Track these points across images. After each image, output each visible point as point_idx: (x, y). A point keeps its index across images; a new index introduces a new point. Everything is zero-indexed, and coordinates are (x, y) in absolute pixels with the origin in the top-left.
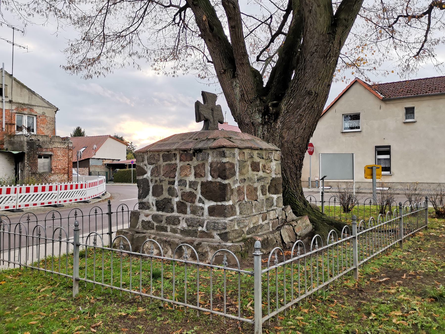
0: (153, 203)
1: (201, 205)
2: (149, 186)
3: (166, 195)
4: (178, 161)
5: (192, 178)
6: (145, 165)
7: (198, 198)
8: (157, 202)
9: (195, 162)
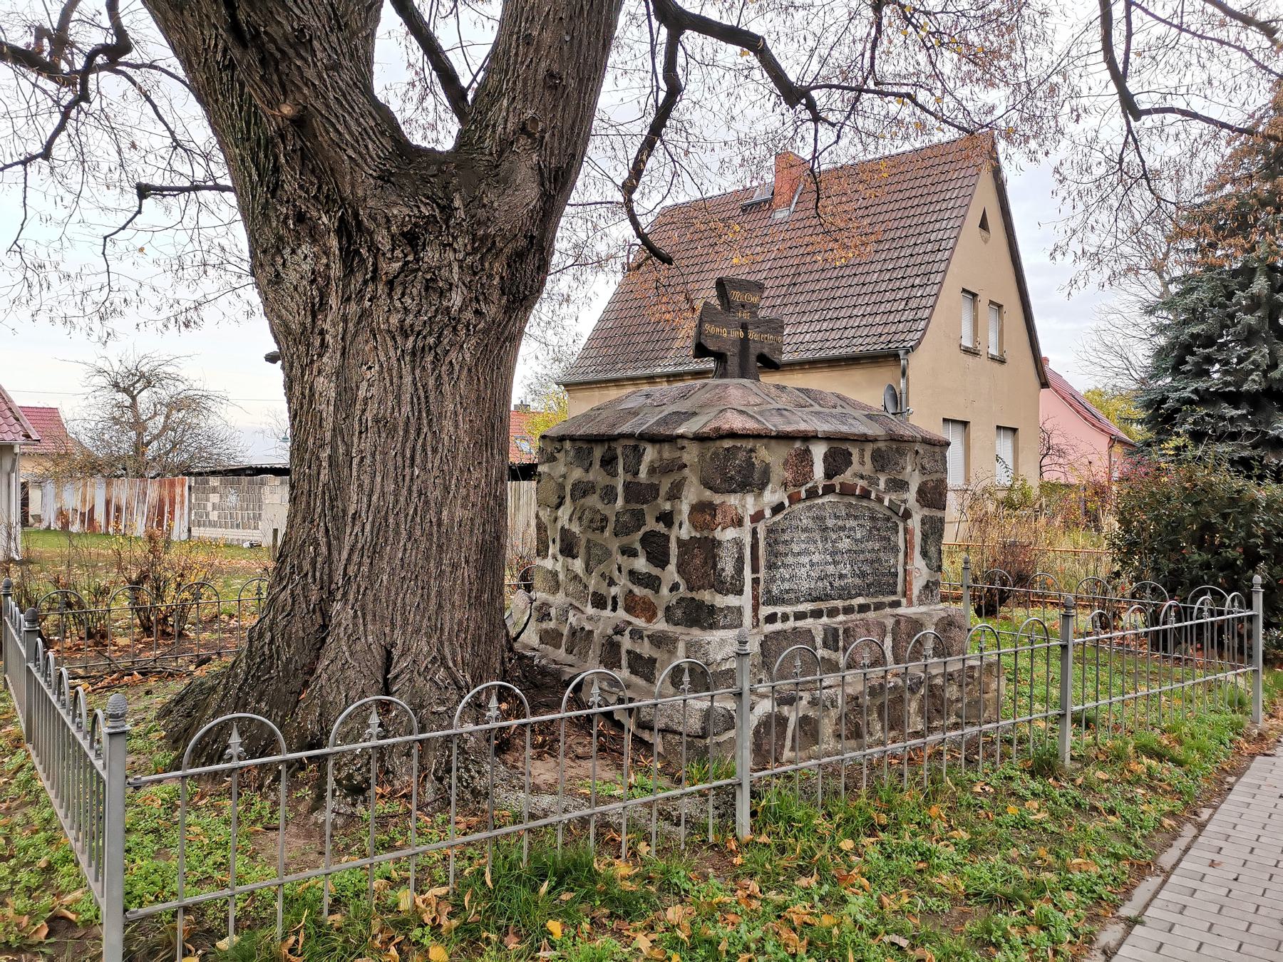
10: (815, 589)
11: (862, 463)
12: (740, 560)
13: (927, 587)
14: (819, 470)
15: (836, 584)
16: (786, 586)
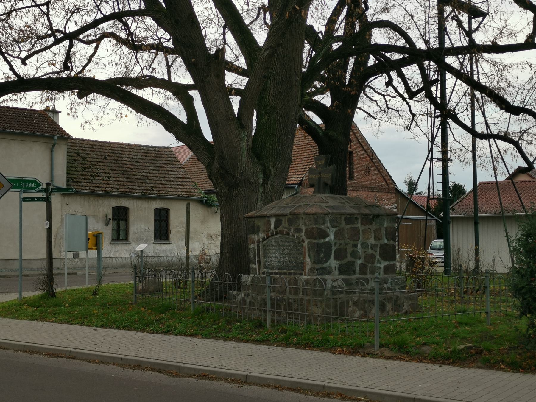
1: (378, 265)
2: (331, 250)
3: (349, 258)
4: (359, 225)
5: (372, 241)
6: (328, 228)
7: (377, 259)
8: (340, 266)
9: (374, 226)
10: (278, 265)
11: (285, 223)
12: (255, 254)
13: (311, 269)
14: (272, 226)
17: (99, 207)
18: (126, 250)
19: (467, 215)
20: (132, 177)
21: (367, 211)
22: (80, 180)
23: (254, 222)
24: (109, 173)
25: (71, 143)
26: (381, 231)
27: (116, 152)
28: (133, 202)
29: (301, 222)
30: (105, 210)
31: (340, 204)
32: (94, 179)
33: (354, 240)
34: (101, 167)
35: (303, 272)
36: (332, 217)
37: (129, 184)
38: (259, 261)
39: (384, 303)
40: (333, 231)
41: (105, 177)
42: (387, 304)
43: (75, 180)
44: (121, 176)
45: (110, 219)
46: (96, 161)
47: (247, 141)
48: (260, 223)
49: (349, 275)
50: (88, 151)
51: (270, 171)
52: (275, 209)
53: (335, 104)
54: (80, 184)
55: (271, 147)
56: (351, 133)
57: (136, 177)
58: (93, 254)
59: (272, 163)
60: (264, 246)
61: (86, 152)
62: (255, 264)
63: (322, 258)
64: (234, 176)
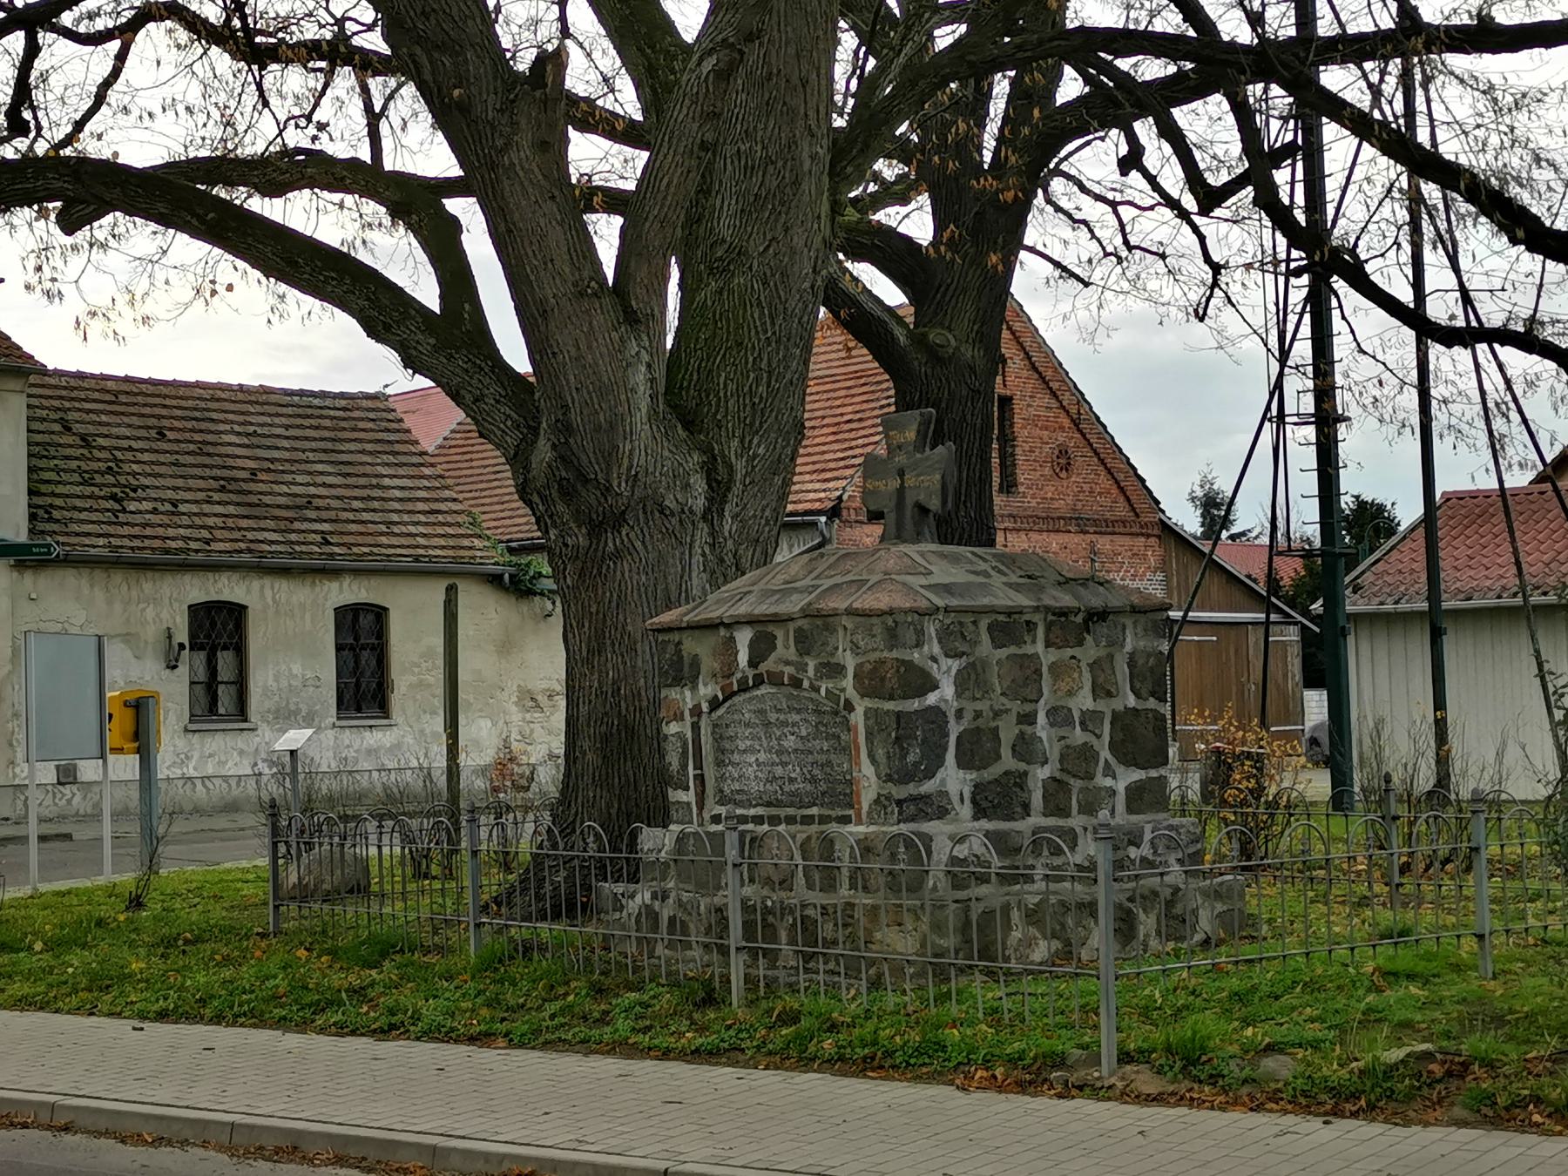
0: (961, 794)
1: (1108, 782)
2: (947, 735)
3: (1008, 761)
4: (1040, 647)
5: (1084, 701)
6: (934, 659)
7: (1102, 763)
8: (978, 788)
9: (1090, 651)
10: (765, 792)
12: (684, 754)
13: (877, 801)
14: (743, 658)
15: (786, 789)
16: (736, 786)
17: (142, 606)
18: (241, 753)
19: (1403, 606)
20: (254, 499)
21: (1066, 600)
22: (76, 515)
23: (680, 643)
24: (175, 489)
25: (43, 386)
26: (1113, 669)
27: (197, 414)
28: (262, 587)
29: (841, 641)
30: (165, 615)
31: (972, 578)
32: (124, 511)
33: (1025, 700)
34: (148, 469)
35: (851, 812)
36: (948, 621)
37: (244, 523)
38: (700, 779)
39: (1129, 911)
40: (949, 669)
41: (163, 501)
42: (1142, 916)
43: (56, 514)
44: (216, 497)
45: (182, 646)
46: (130, 449)
47: (649, 366)
48: (700, 648)
49: (1009, 818)
50: (102, 412)
51: (730, 468)
52: (751, 598)
53: (946, 235)
54: (75, 528)
55: (731, 387)
56: (1005, 334)
57: (267, 499)
58: (125, 767)
59: (735, 443)
60: (715, 726)
61: (94, 417)
62: (687, 789)
63: (916, 764)
64: (609, 489)
